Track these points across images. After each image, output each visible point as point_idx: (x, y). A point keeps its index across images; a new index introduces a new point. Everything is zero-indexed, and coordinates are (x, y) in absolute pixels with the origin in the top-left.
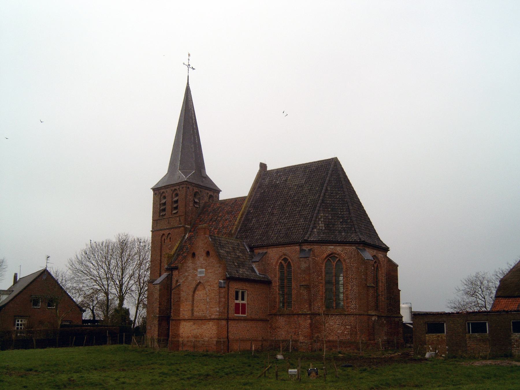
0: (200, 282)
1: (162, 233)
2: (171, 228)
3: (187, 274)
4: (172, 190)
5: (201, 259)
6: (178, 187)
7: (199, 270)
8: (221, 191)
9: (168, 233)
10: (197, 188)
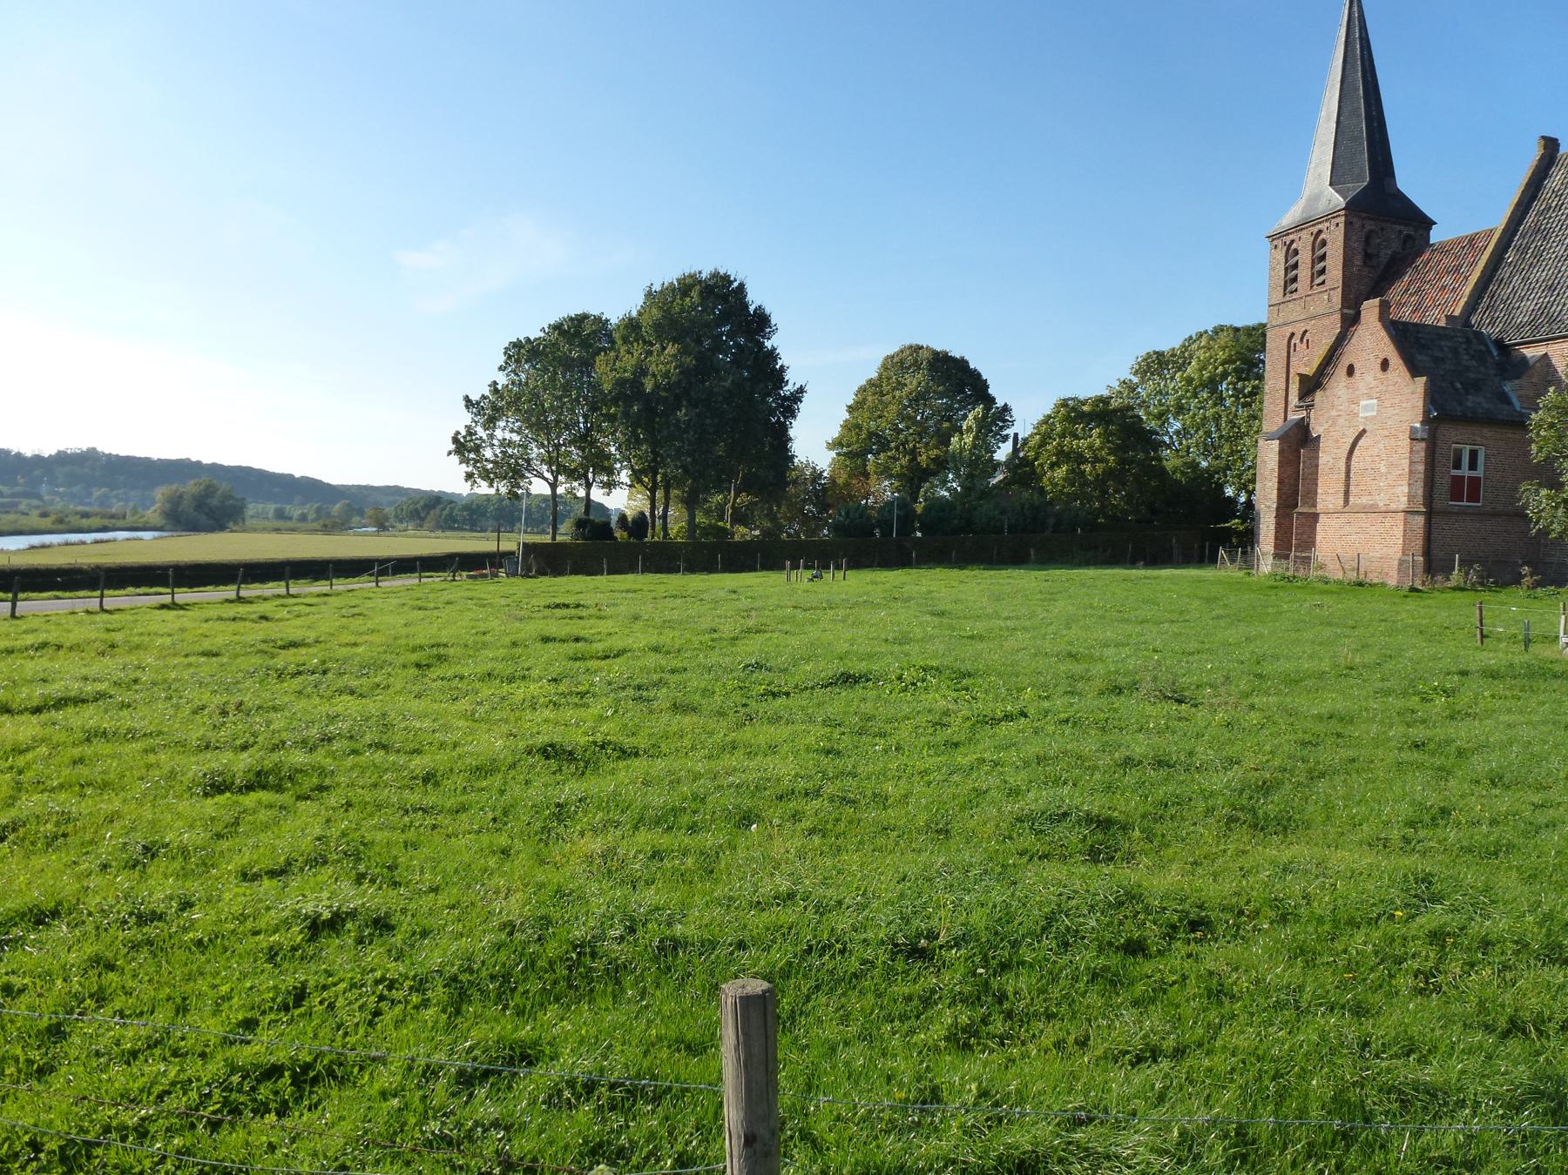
0: (1364, 431)
1: (1289, 330)
3: (1334, 413)
5: (1368, 375)
6: (1327, 224)
7: (1363, 403)
8: (1435, 223)
10: (1373, 223)
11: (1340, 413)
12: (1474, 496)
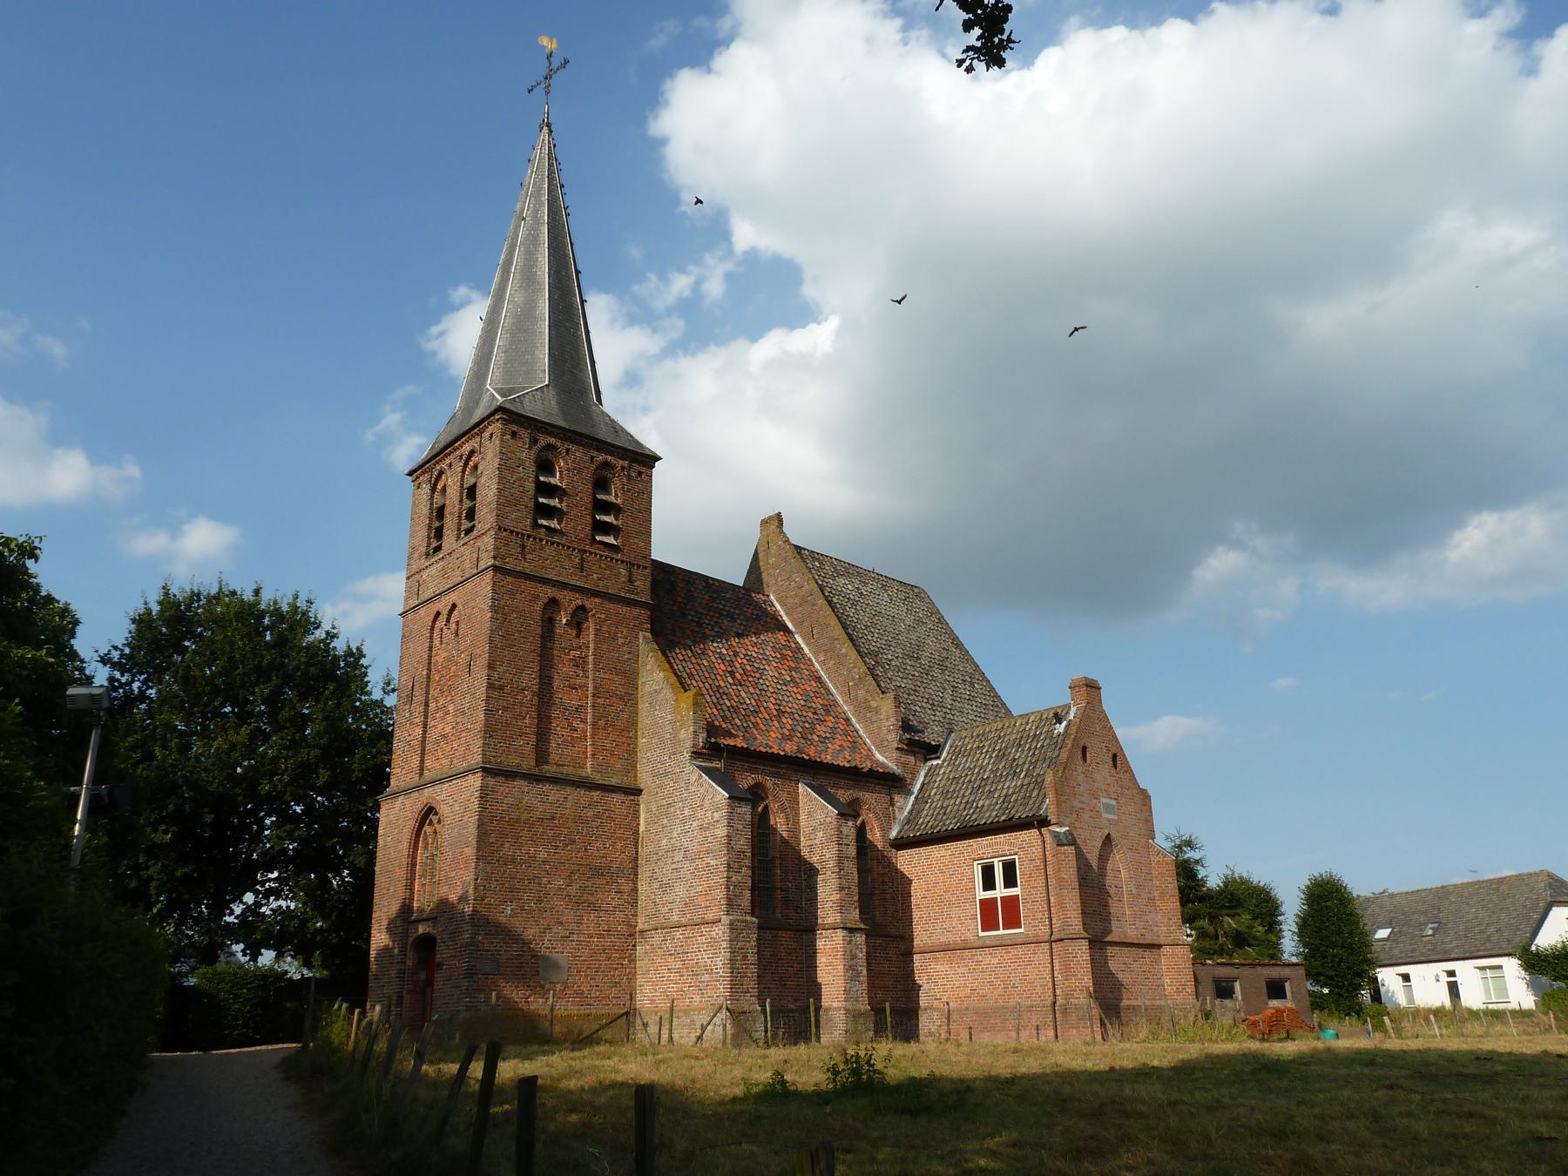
2: (595, 594)
4: (592, 458)
6: (621, 462)
9: (579, 602)
11: (1083, 806)
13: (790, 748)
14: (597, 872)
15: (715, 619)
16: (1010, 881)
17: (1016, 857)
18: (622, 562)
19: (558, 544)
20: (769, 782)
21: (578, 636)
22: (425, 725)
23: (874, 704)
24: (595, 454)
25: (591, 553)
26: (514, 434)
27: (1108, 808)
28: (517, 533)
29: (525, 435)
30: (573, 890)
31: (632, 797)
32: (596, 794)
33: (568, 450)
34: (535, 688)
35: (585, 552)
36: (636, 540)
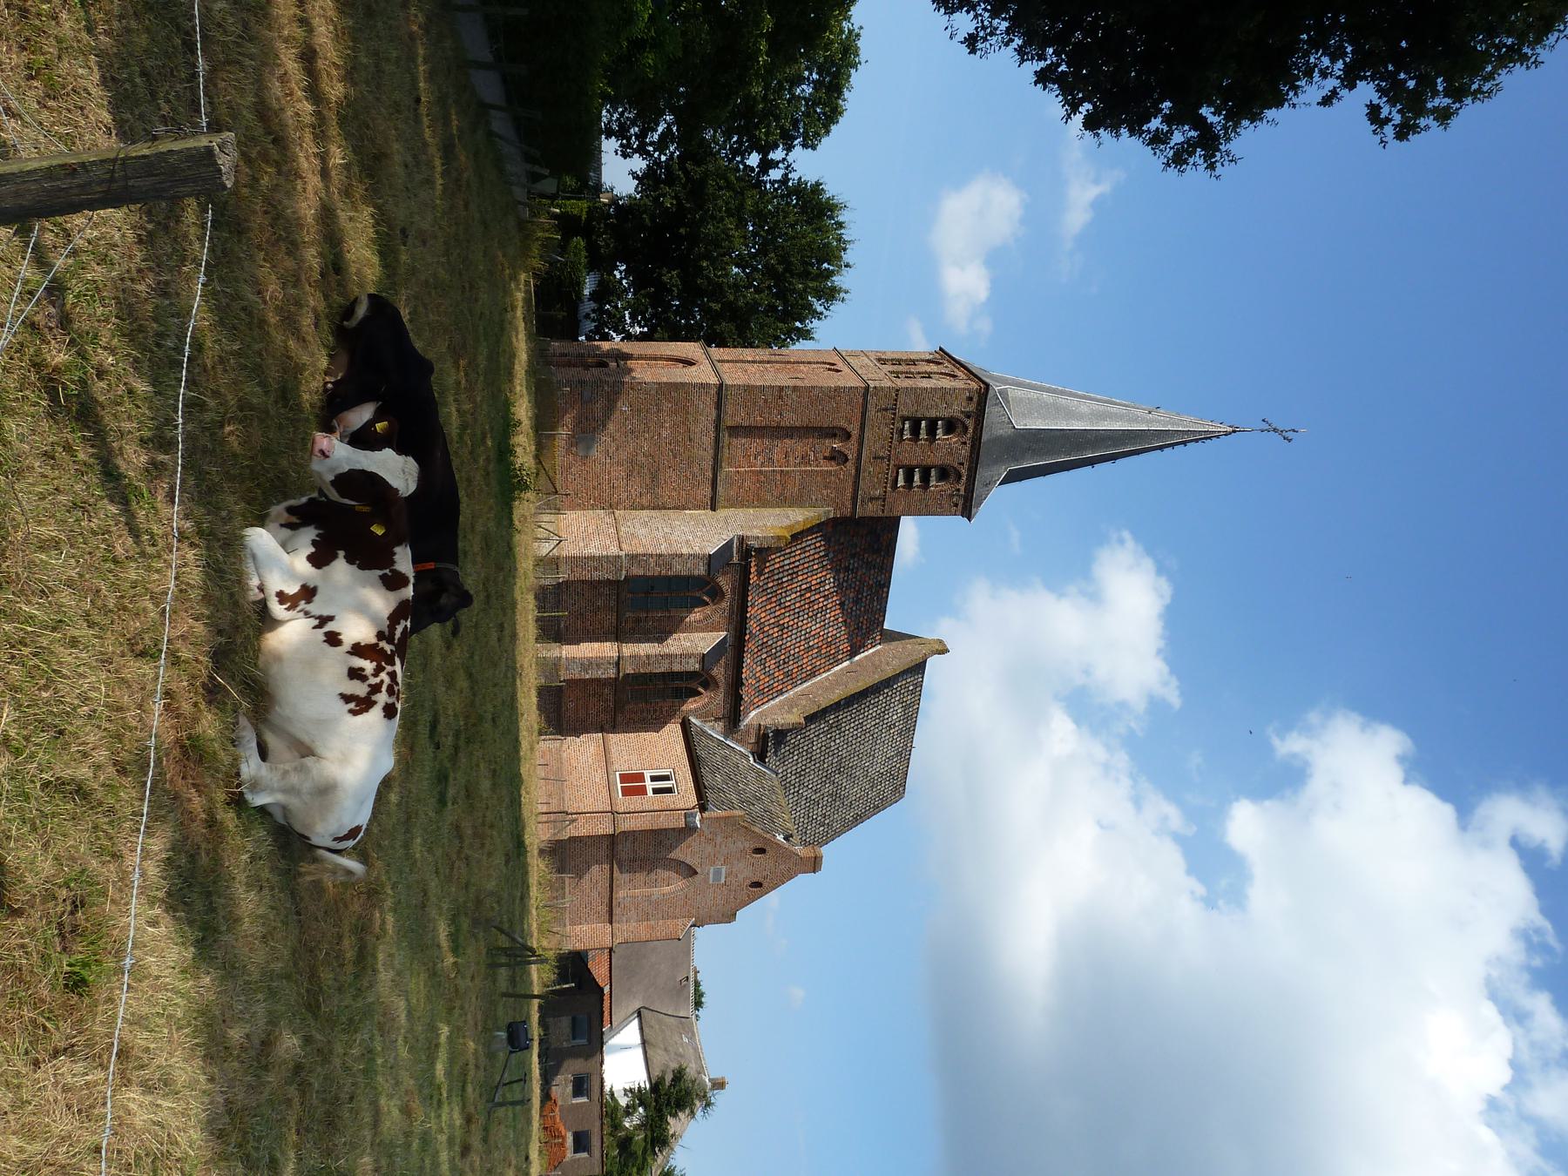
1: (855, 433)
2: (858, 470)
4: (962, 464)
6: (962, 488)
7: (723, 870)
9: (850, 457)
11: (718, 847)
12: (626, 792)
13: (752, 625)
14: (654, 478)
15: (853, 585)
16: (656, 791)
17: (676, 793)
18: (885, 492)
19: (892, 438)
20: (725, 604)
21: (825, 458)
22: (754, 362)
23: (795, 710)
24: (966, 466)
25: (888, 465)
26: (970, 399)
27: (718, 873)
28: (895, 405)
29: (972, 407)
30: (641, 458)
31: (709, 504)
32: (709, 474)
33: (965, 443)
34: (782, 424)
35: (889, 461)
36: (903, 503)
